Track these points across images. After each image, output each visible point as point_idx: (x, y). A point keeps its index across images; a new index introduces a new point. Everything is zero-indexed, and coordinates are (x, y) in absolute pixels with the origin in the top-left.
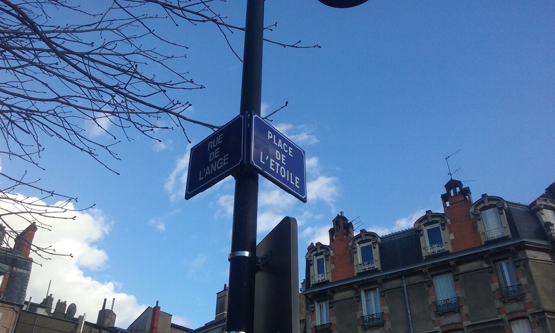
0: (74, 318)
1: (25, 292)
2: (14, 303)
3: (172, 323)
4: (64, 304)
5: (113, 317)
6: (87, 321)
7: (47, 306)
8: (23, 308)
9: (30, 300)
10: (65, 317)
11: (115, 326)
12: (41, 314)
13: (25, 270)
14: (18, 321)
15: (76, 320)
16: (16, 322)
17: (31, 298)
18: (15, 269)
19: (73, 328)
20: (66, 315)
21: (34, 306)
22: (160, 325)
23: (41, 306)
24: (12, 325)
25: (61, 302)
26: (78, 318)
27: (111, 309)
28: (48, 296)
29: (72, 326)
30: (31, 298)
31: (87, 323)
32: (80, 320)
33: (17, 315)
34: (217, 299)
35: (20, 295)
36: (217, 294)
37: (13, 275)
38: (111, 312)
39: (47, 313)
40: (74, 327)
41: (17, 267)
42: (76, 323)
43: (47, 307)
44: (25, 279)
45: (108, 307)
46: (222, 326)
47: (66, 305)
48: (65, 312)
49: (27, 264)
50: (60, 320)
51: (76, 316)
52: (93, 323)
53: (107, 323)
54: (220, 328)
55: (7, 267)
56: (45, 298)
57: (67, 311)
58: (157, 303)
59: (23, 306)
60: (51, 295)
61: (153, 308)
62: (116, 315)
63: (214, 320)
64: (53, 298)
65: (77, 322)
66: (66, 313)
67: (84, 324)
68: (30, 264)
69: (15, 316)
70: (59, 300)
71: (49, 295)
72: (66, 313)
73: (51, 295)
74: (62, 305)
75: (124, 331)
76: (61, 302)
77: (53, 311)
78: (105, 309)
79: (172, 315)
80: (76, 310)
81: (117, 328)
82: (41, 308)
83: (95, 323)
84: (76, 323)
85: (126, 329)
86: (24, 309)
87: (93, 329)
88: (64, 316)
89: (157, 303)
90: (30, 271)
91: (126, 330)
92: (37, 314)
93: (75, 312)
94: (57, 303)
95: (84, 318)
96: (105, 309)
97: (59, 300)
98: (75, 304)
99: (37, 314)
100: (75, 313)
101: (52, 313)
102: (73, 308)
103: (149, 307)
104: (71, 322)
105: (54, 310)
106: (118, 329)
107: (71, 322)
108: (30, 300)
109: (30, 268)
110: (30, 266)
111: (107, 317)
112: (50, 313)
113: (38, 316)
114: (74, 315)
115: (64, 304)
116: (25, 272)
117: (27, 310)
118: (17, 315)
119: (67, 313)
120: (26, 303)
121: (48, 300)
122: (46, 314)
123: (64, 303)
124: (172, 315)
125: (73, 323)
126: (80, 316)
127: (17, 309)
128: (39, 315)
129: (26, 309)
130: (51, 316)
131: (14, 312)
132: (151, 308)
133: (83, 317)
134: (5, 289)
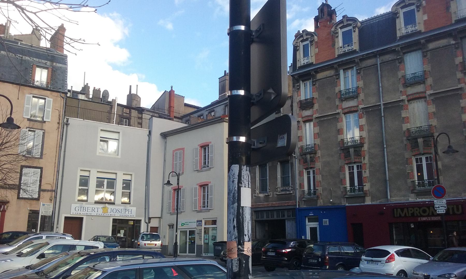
0: (108, 101)
1: (66, 82)
2: (60, 91)
3: (185, 103)
4: (99, 90)
5: (138, 100)
6: (119, 103)
7: (86, 93)
8: (67, 95)
9: (72, 88)
10: (102, 101)
11: (141, 106)
12: (82, 99)
13: (63, 65)
14: (66, 105)
15: (110, 102)
16: (64, 106)
17: (72, 87)
18: (54, 64)
19: (109, 109)
20: (102, 99)
21: (75, 93)
22: (176, 104)
23: (81, 93)
24: (62, 107)
25: (96, 89)
26: (111, 101)
27: (136, 94)
28: (85, 85)
29: (108, 107)
30: (72, 87)
31: (118, 105)
32: (113, 102)
33: (64, 100)
34: (219, 83)
35: (63, 85)
36: (219, 78)
37: (54, 69)
38: (136, 95)
39: (87, 98)
40: (109, 108)
41: (56, 63)
42: (110, 105)
43: (86, 94)
44: (64, 72)
45: (133, 92)
46: (224, 104)
47: (101, 91)
48: (100, 97)
49: (63, 60)
50: (98, 103)
51: (110, 99)
52: (124, 104)
53: (134, 104)
54: (223, 106)
55: (49, 63)
56: (83, 87)
57: (102, 96)
58: (172, 87)
59: (67, 93)
60: (87, 84)
61: (168, 91)
62: (140, 98)
63: (218, 99)
64: (89, 86)
65: (111, 104)
66: (101, 97)
67: (117, 105)
68: (66, 59)
69: (62, 101)
70: (94, 88)
71: (86, 84)
72: (101, 97)
73: (87, 84)
74: (96, 91)
75: (148, 110)
76: (96, 89)
77: (91, 96)
78: (132, 93)
79: (184, 97)
80: (109, 95)
81: (142, 108)
82: (81, 95)
83: (125, 105)
84: (110, 105)
85: (150, 109)
86: (68, 95)
87: (124, 109)
88: (100, 100)
89: (172, 87)
90: (67, 65)
91: (150, 109)
92: (79, 99)
93: (109, 96)
94: (93, 90)
95: (116, 101)
96: (132, 93)
97: (94, 88)
98: (107, 91)
99: (79, 99)
100: (108, 97)
101: (91, 98)
102: (106, 93)
103: (166, 91)
104: (107, 104)
105: (92, 95)
106: (144, 109)
107: (107, 104)
108: (72, 88)
109: (66, 62)
110: (66, 61)
111: (134, 100)
112: (89, 98)
113: (80, 100)
114: (108, 99)
115: (99, 90)
116: (63, 66)
117: (71, 96)
118: (64, 100)
119: (102, 98)
120: (69, 91)
121: (85, 89)
122: (86, 99)
123: (98, 90)
124: (184, 97)
125: (108, 105)
126: (112, 100)
127: (63, 95)
128: (81, 100)
129: (70, 96)
130: (91, 100)
131: (62, 98)
132: (167, 91)
133: (115, 100)
134: (51, 80)
